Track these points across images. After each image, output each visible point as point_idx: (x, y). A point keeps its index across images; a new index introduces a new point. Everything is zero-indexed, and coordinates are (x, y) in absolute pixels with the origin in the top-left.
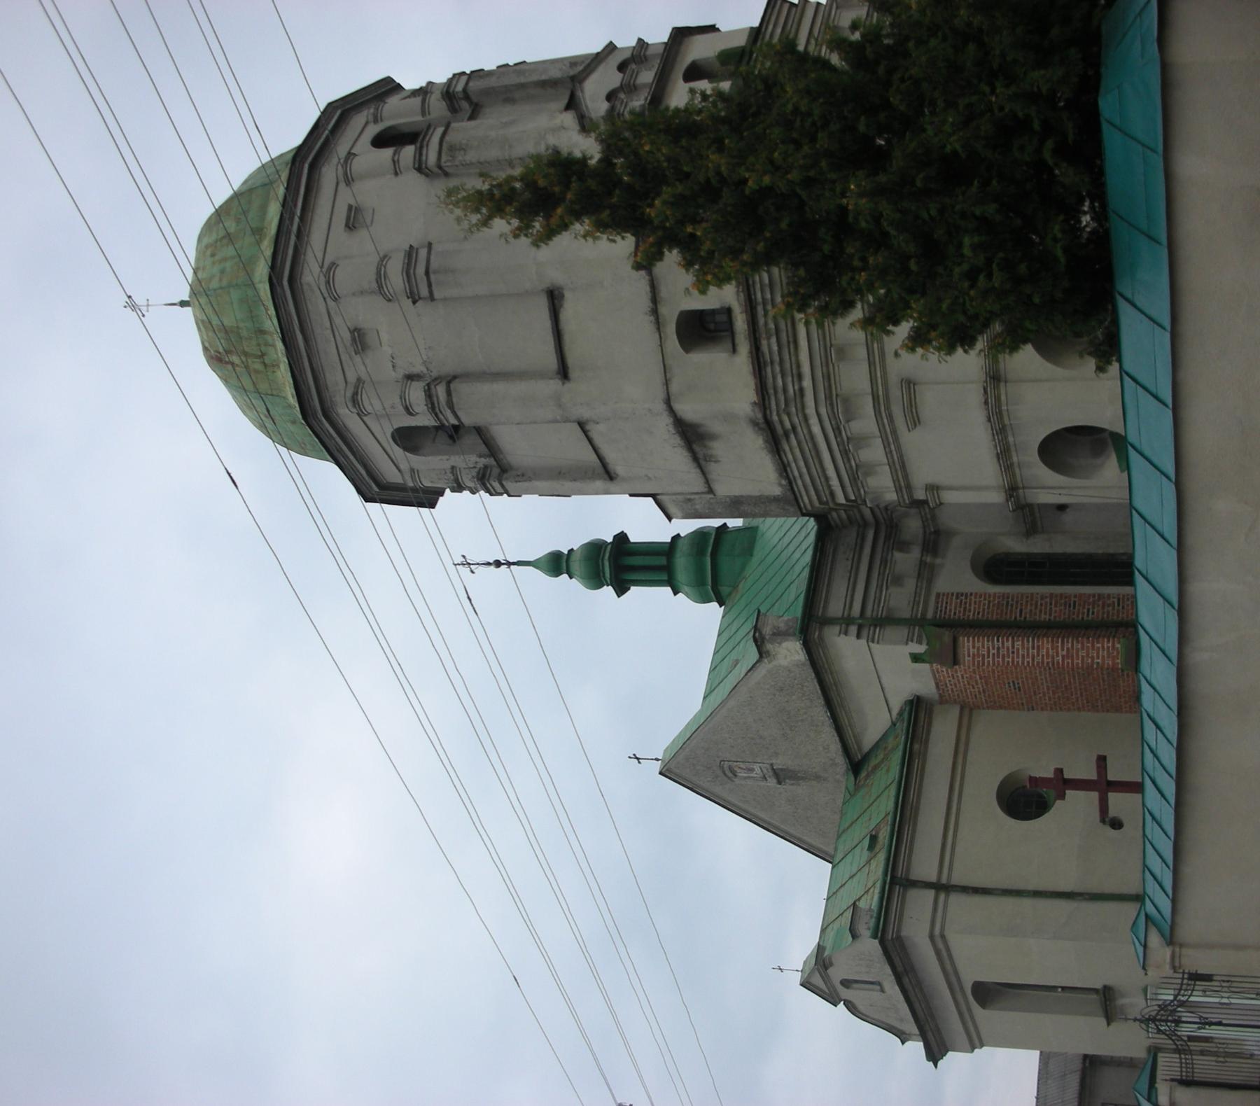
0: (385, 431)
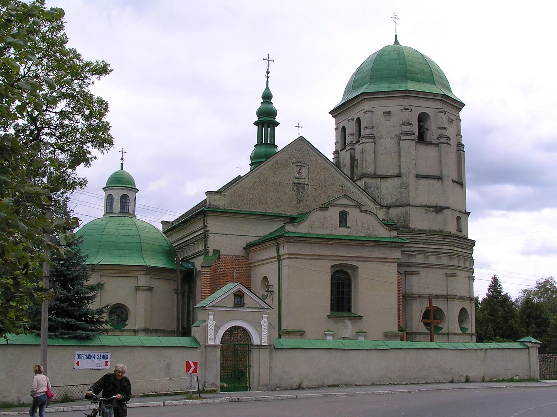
0: (430, 112)
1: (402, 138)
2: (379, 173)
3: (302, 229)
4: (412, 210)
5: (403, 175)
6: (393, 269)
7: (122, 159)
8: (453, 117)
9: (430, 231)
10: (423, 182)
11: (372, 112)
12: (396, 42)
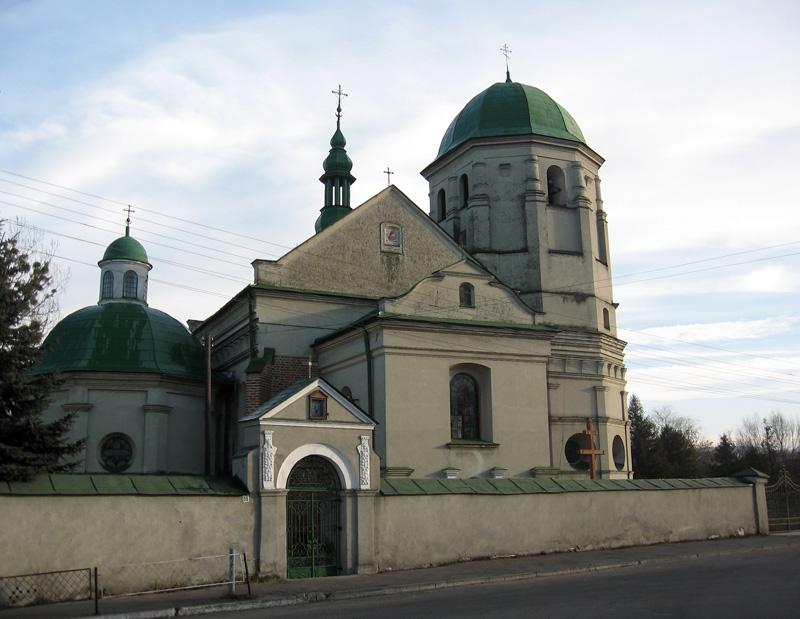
0: (562, 165)
1: (527, 198)
2: (497, 247)
3: (403, 308)
4: (543, 295)
5: (530, 250)
6: (540, 371)
7: (128, 220)
8: (590, 175)
9: (571, 327)
10: (557, 259)
11: (483, 164)
12: (508, 80)
